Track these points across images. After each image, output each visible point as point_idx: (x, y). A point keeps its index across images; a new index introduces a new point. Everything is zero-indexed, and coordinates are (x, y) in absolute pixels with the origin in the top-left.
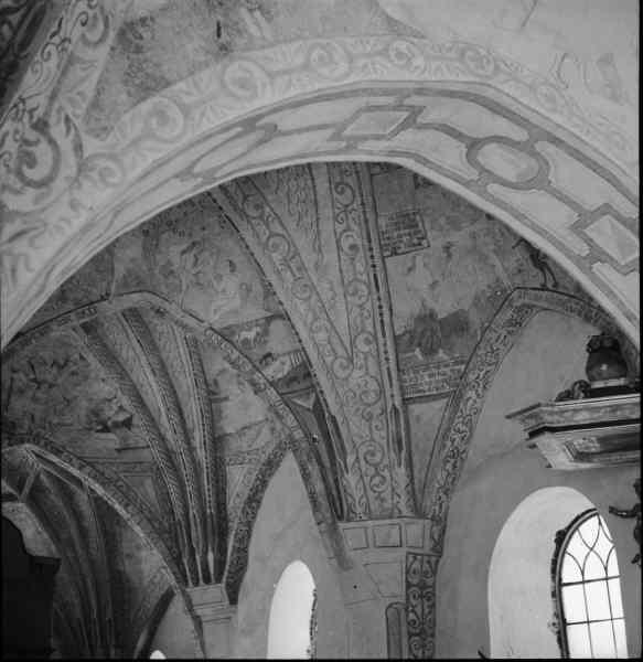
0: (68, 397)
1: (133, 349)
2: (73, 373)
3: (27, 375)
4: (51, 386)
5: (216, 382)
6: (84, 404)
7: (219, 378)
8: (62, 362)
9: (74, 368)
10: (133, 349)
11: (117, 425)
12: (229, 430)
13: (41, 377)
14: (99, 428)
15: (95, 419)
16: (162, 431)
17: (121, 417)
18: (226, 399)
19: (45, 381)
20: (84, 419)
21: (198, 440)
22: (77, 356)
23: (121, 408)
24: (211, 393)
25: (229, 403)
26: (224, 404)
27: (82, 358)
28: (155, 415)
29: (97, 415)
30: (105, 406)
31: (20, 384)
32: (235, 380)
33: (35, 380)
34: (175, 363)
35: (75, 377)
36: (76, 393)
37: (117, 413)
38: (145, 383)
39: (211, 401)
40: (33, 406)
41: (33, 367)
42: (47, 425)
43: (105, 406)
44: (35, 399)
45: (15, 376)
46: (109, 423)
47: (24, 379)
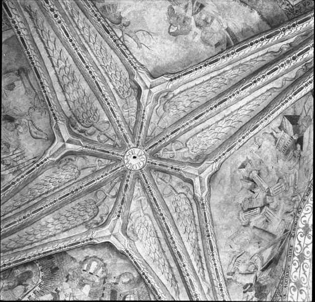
0: (277, 178)
1: (217, 122)
2: (259, 174)
3: (256, 214)
4: (268, 194)
5: (217, 45)
6: (281, 162)
7: (214, 42)
8: (250, 184)
9: (255, 174)
10: (217, 122)
11: (296, 131)
12: (255, 16)
13: (261, 203)
14: (299, 146)
15: (291, 152)
16: (288, 83)
17: (289, 126)
18: (228, 30)
19: (265, 199)
20: (292, 163)
21: (280, 45)
22: (243, 170)
23: (281, 128)
24: (229, 46)
25: (231, 26)
26: (236, 31)
27: (243, 166)
28: (275, 94)
29: (288, 151)
30: (282, 143)
31: (261, 221)
32: (208, 29)
33: (262, 208)
34: (215, 85)
35: (262, 171)
36: (274, 171)
37: (285, 131)
38: (247, 107)
39: (237, 43)
40: (280, 211)
41: (249, 209)
42: (294, 199)
43: (282, 143)
44: (275, 210)
45: (252, 225)
46: (295, 138)
47: (258, 217)
